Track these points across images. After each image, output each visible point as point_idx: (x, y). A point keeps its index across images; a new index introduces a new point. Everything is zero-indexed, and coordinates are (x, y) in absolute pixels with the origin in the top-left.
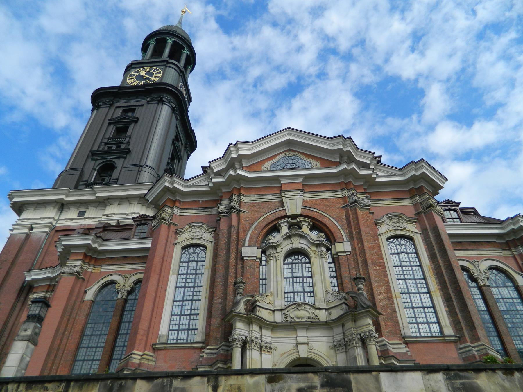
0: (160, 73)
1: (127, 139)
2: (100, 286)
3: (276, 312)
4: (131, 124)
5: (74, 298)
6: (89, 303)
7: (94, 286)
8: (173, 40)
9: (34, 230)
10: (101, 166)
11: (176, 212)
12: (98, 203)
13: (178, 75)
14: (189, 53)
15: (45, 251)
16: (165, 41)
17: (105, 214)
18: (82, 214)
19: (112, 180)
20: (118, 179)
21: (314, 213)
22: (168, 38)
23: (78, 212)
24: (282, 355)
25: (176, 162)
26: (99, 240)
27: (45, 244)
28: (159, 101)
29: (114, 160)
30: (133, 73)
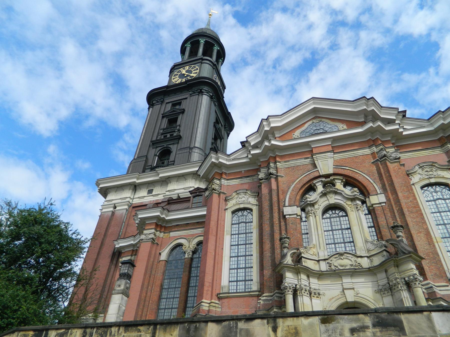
0: (197, 69)
1: (178, 128)
2: (171, 248)
3: (321, 262)
4: (179, 115)
5: (152, 260)
6: (164, 263)
7: (166, 248)
8: (205, 40)
9: (117, 208)
10: (161, 152)
11: (223, 182)
12: (162, 182)
13: (212, 68)
14: (219, 48)
15: (126, 224)
16: (198, 42)
17: (167, 190)
18: (150, 192)
19: (170, 162)
20: (174, 161)
21: (345, 171)
22: (200, 40)
23: (147, 191)
24: (330, 300)
25: (219, 141)
26: (166, 212)
27: (126, 219)
28: (199, 93)
29: (169, 146)
30: (176, 73)
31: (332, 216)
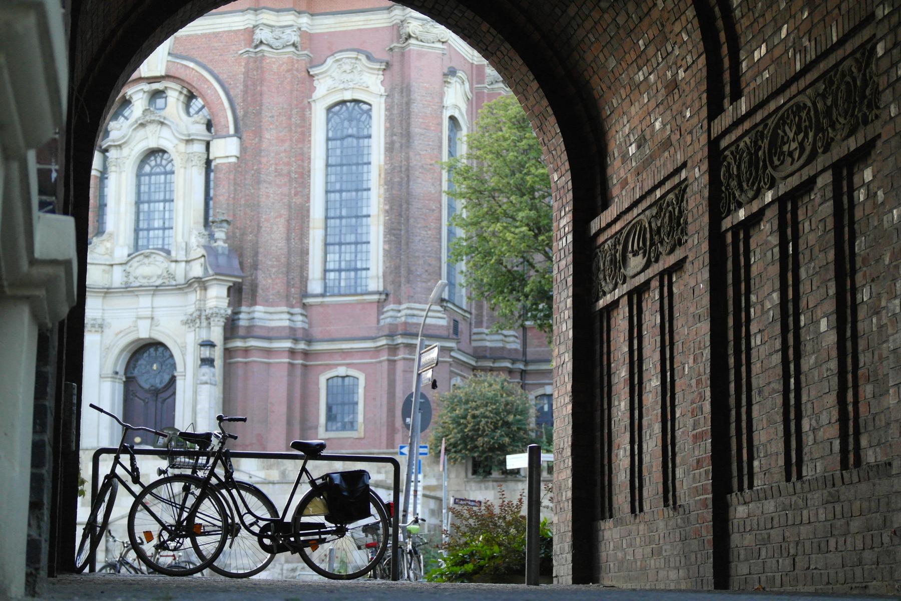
3: (115, 267)
24: (117, 334)
31: (153, 171)
